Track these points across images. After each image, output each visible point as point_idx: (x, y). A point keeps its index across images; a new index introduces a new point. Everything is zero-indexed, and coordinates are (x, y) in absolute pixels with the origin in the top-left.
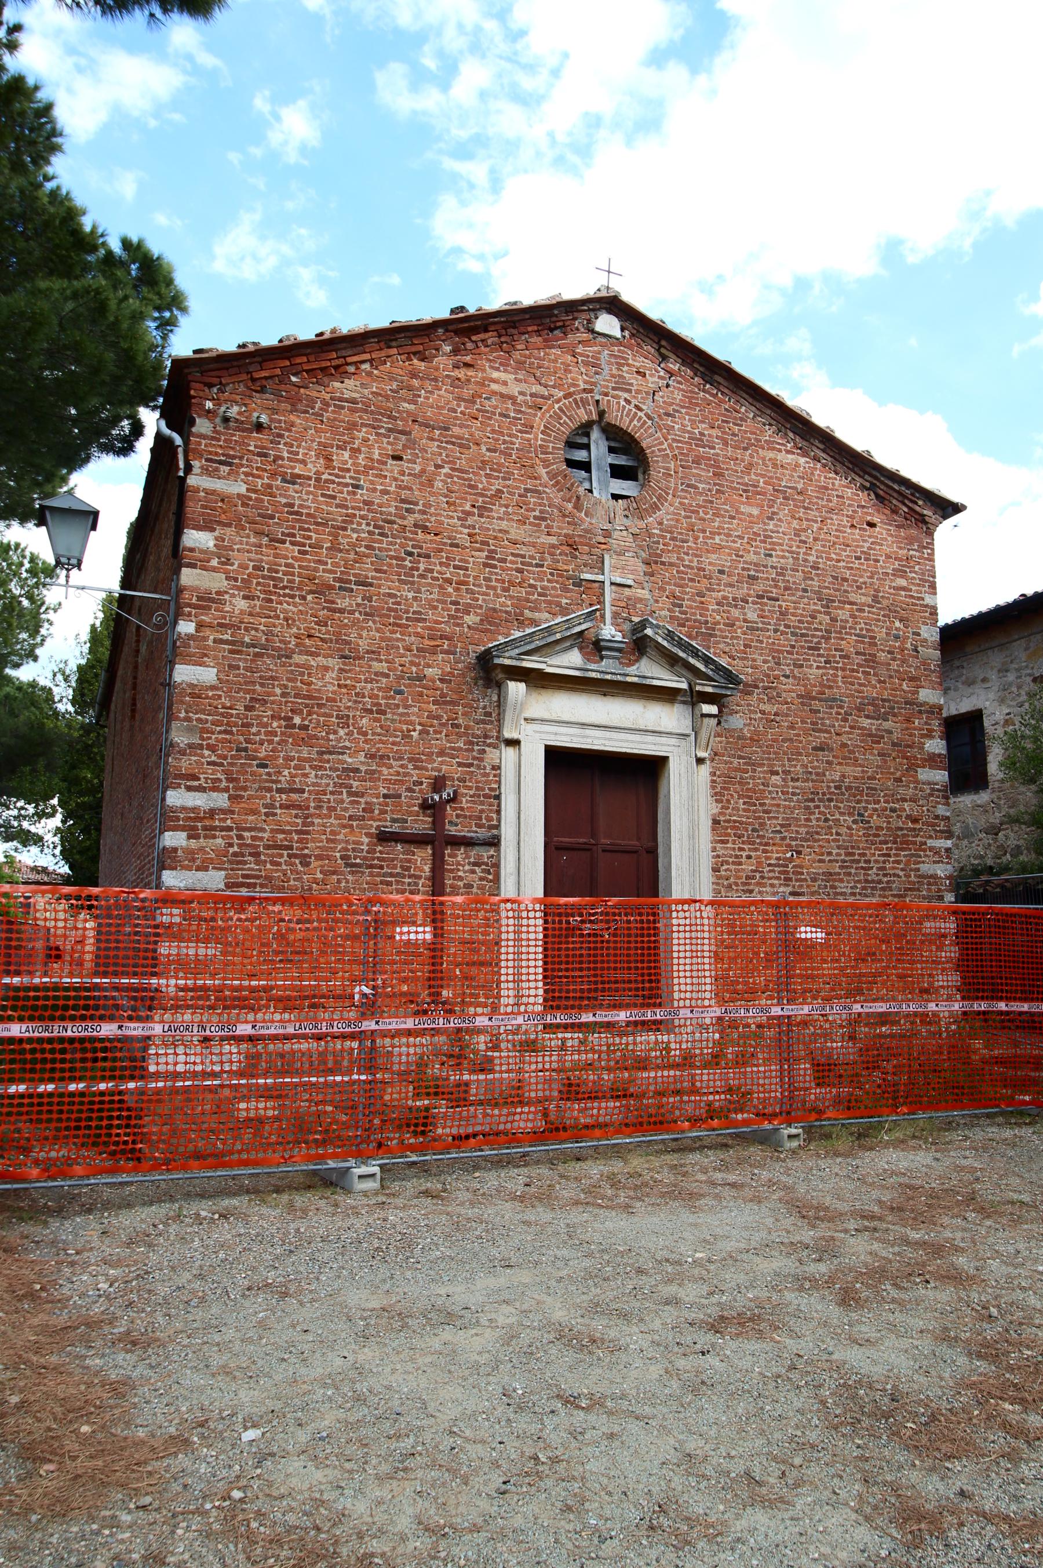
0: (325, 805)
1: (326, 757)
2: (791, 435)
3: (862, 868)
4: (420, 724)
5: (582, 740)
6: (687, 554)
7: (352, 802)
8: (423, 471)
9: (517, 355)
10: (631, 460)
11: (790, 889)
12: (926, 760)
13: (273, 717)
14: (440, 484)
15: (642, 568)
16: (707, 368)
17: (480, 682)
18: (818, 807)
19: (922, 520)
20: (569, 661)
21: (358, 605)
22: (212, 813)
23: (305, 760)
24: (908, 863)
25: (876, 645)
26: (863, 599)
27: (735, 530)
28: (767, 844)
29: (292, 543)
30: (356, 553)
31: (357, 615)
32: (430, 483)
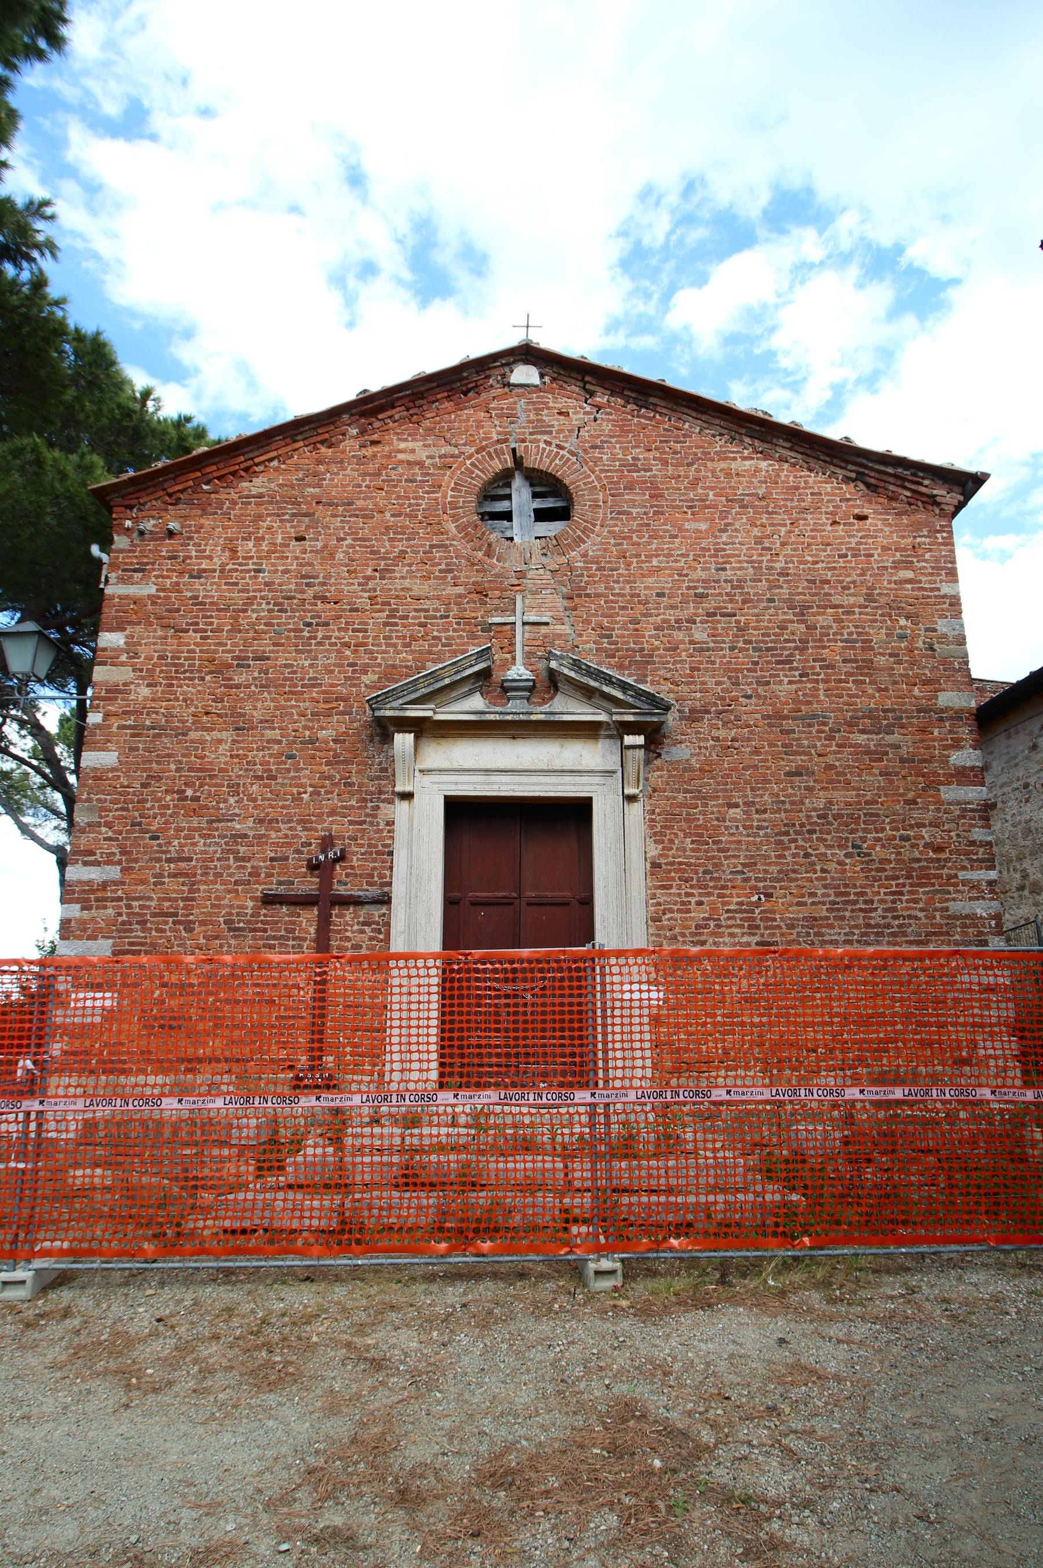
0: (211, 872)
1: (215, 825)
2: (748, 440)
3: (861, 910)
4: (311, 786)
5: (487, 787)
6: (618, 582)
7: (238, 868)
8: (325, 546)
9: (427, 423)
10: (555, 501)
11: (757, 938)
12: (952, 775)
13: (167, 791)
14: (341, 556)
15: (561, 603)
16: (639, 392)
17: (377, 739)
18: (795, 841)
19: (932, 501)
20: (473, 705)
21: (254, 679)
22: (104, 885)
23: (195, 830)
24: (930, 901)
25: (872, 649)
26: (852, 600)
27: (678, 549)
28: (723, 887)
29: (195, 631)
30: (256, 632)
31: (253, 688)
32: (332, 556)
